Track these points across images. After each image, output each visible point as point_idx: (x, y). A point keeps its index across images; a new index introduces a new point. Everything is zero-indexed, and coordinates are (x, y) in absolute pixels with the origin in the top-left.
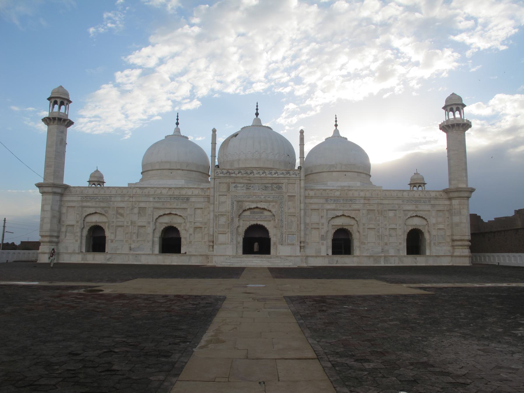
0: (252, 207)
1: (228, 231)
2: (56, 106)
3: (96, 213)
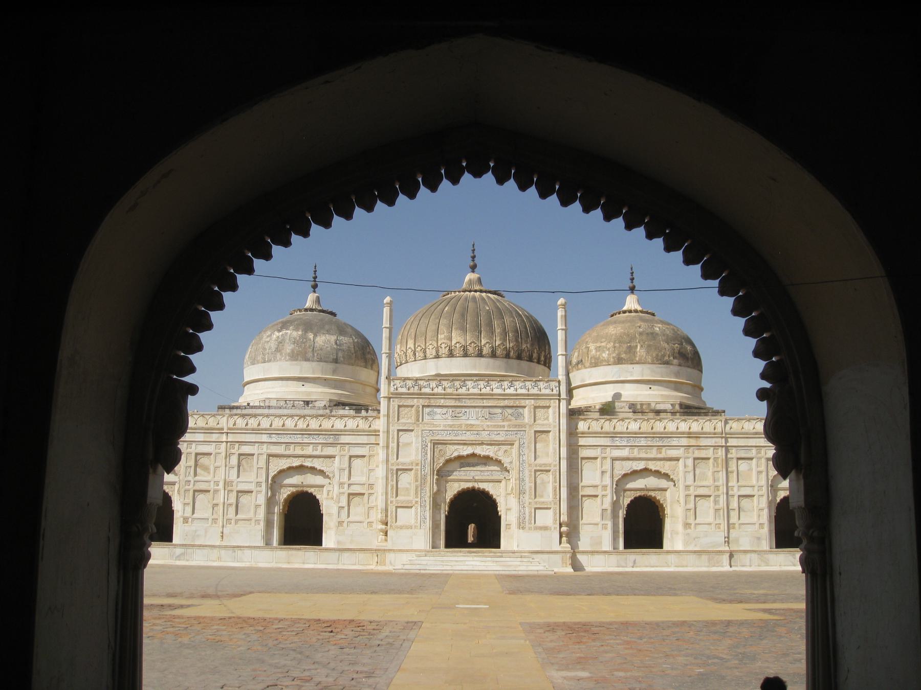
0: (465, 453)
1: (416, 502)
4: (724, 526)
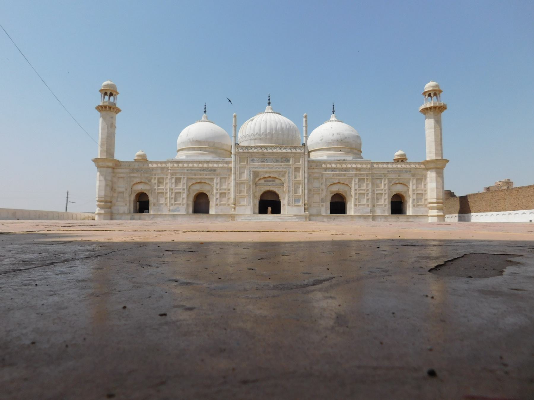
2: (107, 97)
3: (141, 182)
4: (371, 206)
